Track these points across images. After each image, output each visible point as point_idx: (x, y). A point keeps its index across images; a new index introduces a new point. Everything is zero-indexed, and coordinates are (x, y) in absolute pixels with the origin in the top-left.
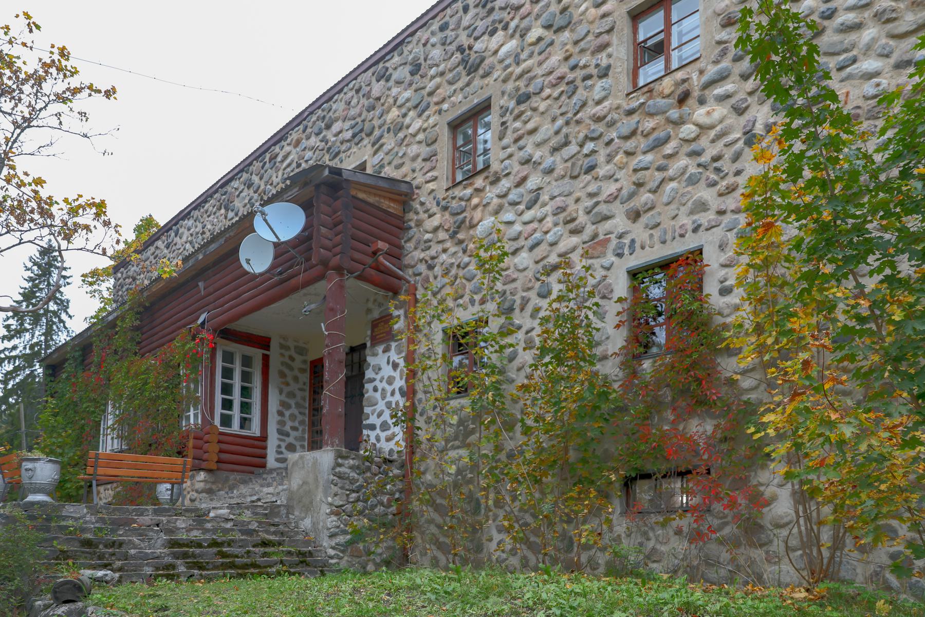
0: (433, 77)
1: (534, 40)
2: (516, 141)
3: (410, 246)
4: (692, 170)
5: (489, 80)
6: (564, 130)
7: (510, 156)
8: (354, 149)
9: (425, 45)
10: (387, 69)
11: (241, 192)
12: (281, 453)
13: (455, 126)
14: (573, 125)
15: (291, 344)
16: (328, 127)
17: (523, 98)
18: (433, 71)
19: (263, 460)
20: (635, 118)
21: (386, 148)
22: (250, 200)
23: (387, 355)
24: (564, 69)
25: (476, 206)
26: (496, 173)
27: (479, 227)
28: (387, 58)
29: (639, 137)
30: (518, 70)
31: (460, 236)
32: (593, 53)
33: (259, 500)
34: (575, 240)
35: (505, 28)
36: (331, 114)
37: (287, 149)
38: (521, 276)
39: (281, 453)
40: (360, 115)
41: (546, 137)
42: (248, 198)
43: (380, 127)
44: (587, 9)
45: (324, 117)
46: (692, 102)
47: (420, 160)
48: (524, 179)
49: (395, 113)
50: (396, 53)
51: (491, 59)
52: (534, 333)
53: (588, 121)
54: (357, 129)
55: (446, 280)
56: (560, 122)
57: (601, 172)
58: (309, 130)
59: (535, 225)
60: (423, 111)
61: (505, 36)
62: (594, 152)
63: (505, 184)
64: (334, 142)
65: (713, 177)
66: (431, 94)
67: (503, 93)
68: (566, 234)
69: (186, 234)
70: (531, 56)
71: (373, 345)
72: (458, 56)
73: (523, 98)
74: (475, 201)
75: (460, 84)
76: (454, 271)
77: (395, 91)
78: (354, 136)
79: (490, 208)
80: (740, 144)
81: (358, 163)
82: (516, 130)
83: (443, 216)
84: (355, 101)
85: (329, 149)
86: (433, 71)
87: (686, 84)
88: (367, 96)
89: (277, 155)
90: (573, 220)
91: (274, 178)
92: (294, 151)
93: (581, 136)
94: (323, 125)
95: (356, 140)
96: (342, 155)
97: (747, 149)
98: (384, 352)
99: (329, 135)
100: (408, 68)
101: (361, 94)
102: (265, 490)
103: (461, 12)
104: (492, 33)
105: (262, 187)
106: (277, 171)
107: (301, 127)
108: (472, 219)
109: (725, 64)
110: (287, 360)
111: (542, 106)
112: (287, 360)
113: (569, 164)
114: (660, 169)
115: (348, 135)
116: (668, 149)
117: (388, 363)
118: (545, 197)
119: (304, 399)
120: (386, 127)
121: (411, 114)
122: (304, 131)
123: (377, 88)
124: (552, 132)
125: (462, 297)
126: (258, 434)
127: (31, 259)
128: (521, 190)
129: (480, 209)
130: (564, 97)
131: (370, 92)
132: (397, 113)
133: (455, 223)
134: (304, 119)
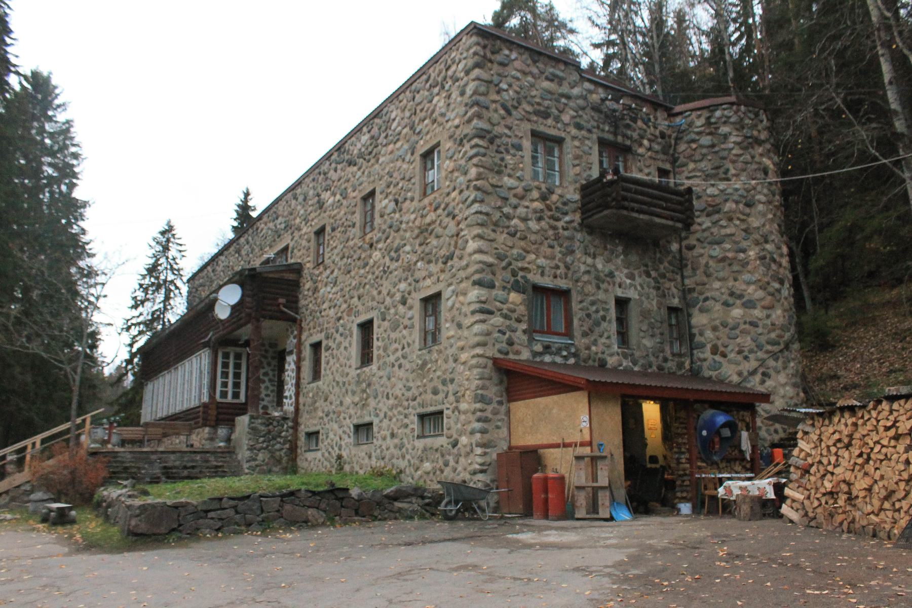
3: (301, 296)
15: (266, 343)
63: (328, 272)
69: (222, 265)
110: (263, 353)
112: (263, 353)
119: (274, 375)
127: (154, 239)
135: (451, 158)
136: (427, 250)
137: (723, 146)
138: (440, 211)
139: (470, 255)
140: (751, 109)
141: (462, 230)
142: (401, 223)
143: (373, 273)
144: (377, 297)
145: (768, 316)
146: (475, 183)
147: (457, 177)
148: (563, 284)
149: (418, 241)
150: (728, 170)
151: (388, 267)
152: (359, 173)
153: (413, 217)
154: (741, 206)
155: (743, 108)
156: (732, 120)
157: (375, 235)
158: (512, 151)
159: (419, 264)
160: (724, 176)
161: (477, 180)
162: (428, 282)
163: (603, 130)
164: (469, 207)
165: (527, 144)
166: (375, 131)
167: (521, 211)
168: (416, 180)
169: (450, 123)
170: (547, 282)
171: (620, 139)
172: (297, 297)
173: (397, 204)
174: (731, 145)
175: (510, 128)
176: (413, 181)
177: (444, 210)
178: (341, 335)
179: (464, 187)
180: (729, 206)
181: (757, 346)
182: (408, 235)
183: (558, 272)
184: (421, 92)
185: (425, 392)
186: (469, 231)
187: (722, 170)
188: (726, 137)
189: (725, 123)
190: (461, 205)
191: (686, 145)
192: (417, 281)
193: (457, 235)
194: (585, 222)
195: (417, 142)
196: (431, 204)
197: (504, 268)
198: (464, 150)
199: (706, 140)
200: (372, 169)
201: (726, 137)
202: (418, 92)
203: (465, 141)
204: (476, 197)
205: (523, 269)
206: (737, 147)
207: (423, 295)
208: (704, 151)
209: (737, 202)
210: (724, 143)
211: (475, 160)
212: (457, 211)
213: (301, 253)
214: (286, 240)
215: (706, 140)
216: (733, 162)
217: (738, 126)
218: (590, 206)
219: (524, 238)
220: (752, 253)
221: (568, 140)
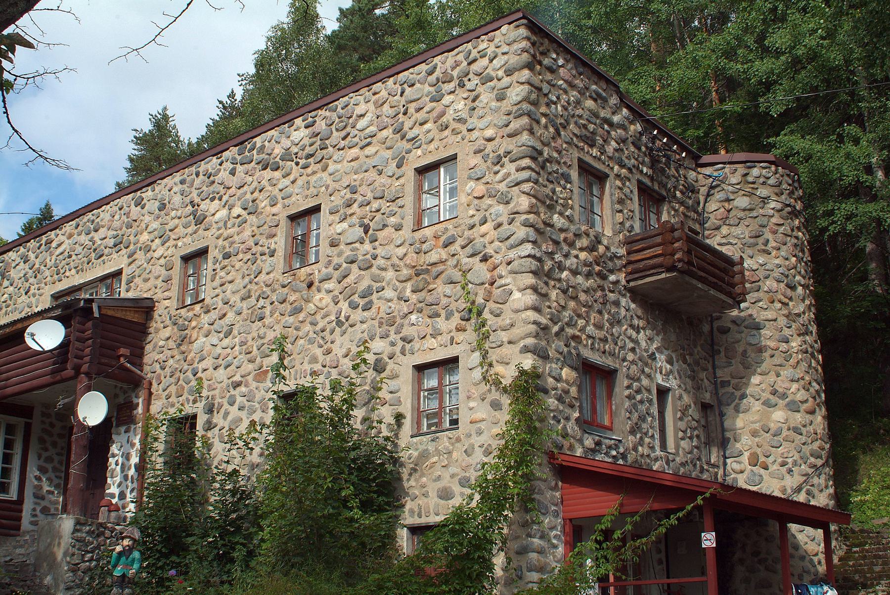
0: (173, 218)
1: (236, 216)
2: (221, 285)
3: (148, 348)
4: (311, 335)
5: (208, 233)
6: (249, 287)
7: (217, 296)
8: (115, 256)
9: (169, 191)
10: (143, 199)
11: (17, 265)
12: (35, 516)
13: (186, 259)
14: (254, 284)
16: (96, 231)
17: (227, 256)
18: (173, 213)
19: (16, 523)
20: (286, 290)
21: (138, 263)
22: (25, 275)
23: (127, 434)
24: (251, 243)
25: (194, 328)
26: (208, 306)
27: (195, 344)
28: (144, 190)
29: (288, 304)
30: (226, 233)
31: (183, 348)
32: (267, 238)
33: (11, 560)
34: (251, 366)
35: (220, 199)
36: (98, 220)
37: (62, 238)
38: (219, 386)
39: (35, 516)
40: (121, 229)
41: (238, 289)
42: (23, 272)
43: (134, 244)
44: (266, 206)
45: (93, 221)
46: (314, 288)
47: (161, 279)
48: (224, 315)
49: (145, 237)
50: (149, 188)
51: (211, 218)
52: (224, 431)
53: (262, 284)
54: (118, 240)
55: (173, 380)
56: (247, 280)
57: (267, 321)
58: (80, 228)
59: (229, 350)
60: (165, 242)
61: (220, 205)
62: (263, 307)
63: (214, 315)
64: (100, 245)
65: (321, 342)
66: (171, 230)
67: (216, 247)
68: (246, 362)
70: (234, 225)
71: (118, 426)
72: (190, 207)
73: (227, 256)
74: (194, 324)
75: (190, 230)
76: (178, 374)
77: (147, 218)
78: (115, 246)
79: (203, 331)
80: (334, 323)
81: (117, 268)
82: (221, 278)
83: (173, 329)
84: (117, 217)
85: (95, 250)
86: (173, 213)
87: (312, 276)
88: (127, 214)
89: (52, 241)
90: (250, 353)
91: (48, 261)
92: (67, 241)
93: (257, 294)
94: (92, 227)
95: (117, 248)
96: (104, 257)
97: (337, 328)
98: (125, 432)
99: (97, 236)
100: (157, 204)
101: (122, 212)
102: (18, 551)
103: (194, 176)
104: (213, 199)
105: (37, 266)
106: (51, 255)
107: (74, 223)
108: (191, 337)
109: (330, 269)
111: (238, 265)
113: (250, 311)
114: (297, 329)
115: (111, 242)
116: (301, 316)
117: (128, 442)
118: (235, 332)
120: (139, 245)
121: (158, 241)
122: (76, 228)
123: (135, 211)
124: (241, 286)
125: (181, 396)
126: (15, 498)
128: (222, 322)
129: (197, 329)
130: (249, 263)
131: (129, 213)
132: (147, 237)
133: (180, 337)
134: (78, 218)
135: (478, 179)
136: (430, 299)
138: (456, 247)
139: (517, 311)
140: (787, 172)
141: (501, 277)
142: (375, 257)
143: (314, 324)
144: (321, 358)
145: (811, 423)
146: (524, 217)
147: (490, 206)
148: (609, 362)
149: (409, 286)
151: (347, 318)
152: (287, 181)
153: (401, 251)
154: (782, 285)
156: (772, 181)
157: (317, 271)
158: (562, 182)
159: (413, 317)
160: (763, 248)
161: (529, 212)
162: (431, 342)
163: (642, 172)
164: (512, 247)
165: (574, 174)
166: (321, 125)
167: (571, 262)
168: (408, 200)
169: (475, 134)
170: (595, 358)
171: (656, 187)
172: (143, 348)
173: (366, 232)
175: (559, 152)
176: (400, 202)
177: (463, 247)
178: (241, 408)
179: (504, 219)
180: (770, 284)
181: (801, 458)
182: (390, 274)
184: (418, 85)
185: (425, 495)
186: (514, 279)
187: (761, 240)
188: (765, 200)
189: (764, 183)
190: (497, 243)
191: (718, 204)
192: (407, 340)
193: (492, 284)
194: (632, 284)
195: (409, 152)
196: (436, 237)
197: (557, 334)
198: (504, 171)
199: (742, 202)
200: (313, 179)
201: (765, 200)
202: (413, 85)
203: (505, 160)
204: (528, 235)
205: (574, 337)
206: (776, 214)
207: (420, 360)
208: (741, 214)
209: (779, 281)
210: (762, 208)
211: (527, 187)
212: (490, 250)
213: (149, 284)
214: (117, 262)
215: (742, 202)
216: (775, 232)
217: (776, 190)
219: (575, 298)
220: (794, 344)
221: (612, 176)
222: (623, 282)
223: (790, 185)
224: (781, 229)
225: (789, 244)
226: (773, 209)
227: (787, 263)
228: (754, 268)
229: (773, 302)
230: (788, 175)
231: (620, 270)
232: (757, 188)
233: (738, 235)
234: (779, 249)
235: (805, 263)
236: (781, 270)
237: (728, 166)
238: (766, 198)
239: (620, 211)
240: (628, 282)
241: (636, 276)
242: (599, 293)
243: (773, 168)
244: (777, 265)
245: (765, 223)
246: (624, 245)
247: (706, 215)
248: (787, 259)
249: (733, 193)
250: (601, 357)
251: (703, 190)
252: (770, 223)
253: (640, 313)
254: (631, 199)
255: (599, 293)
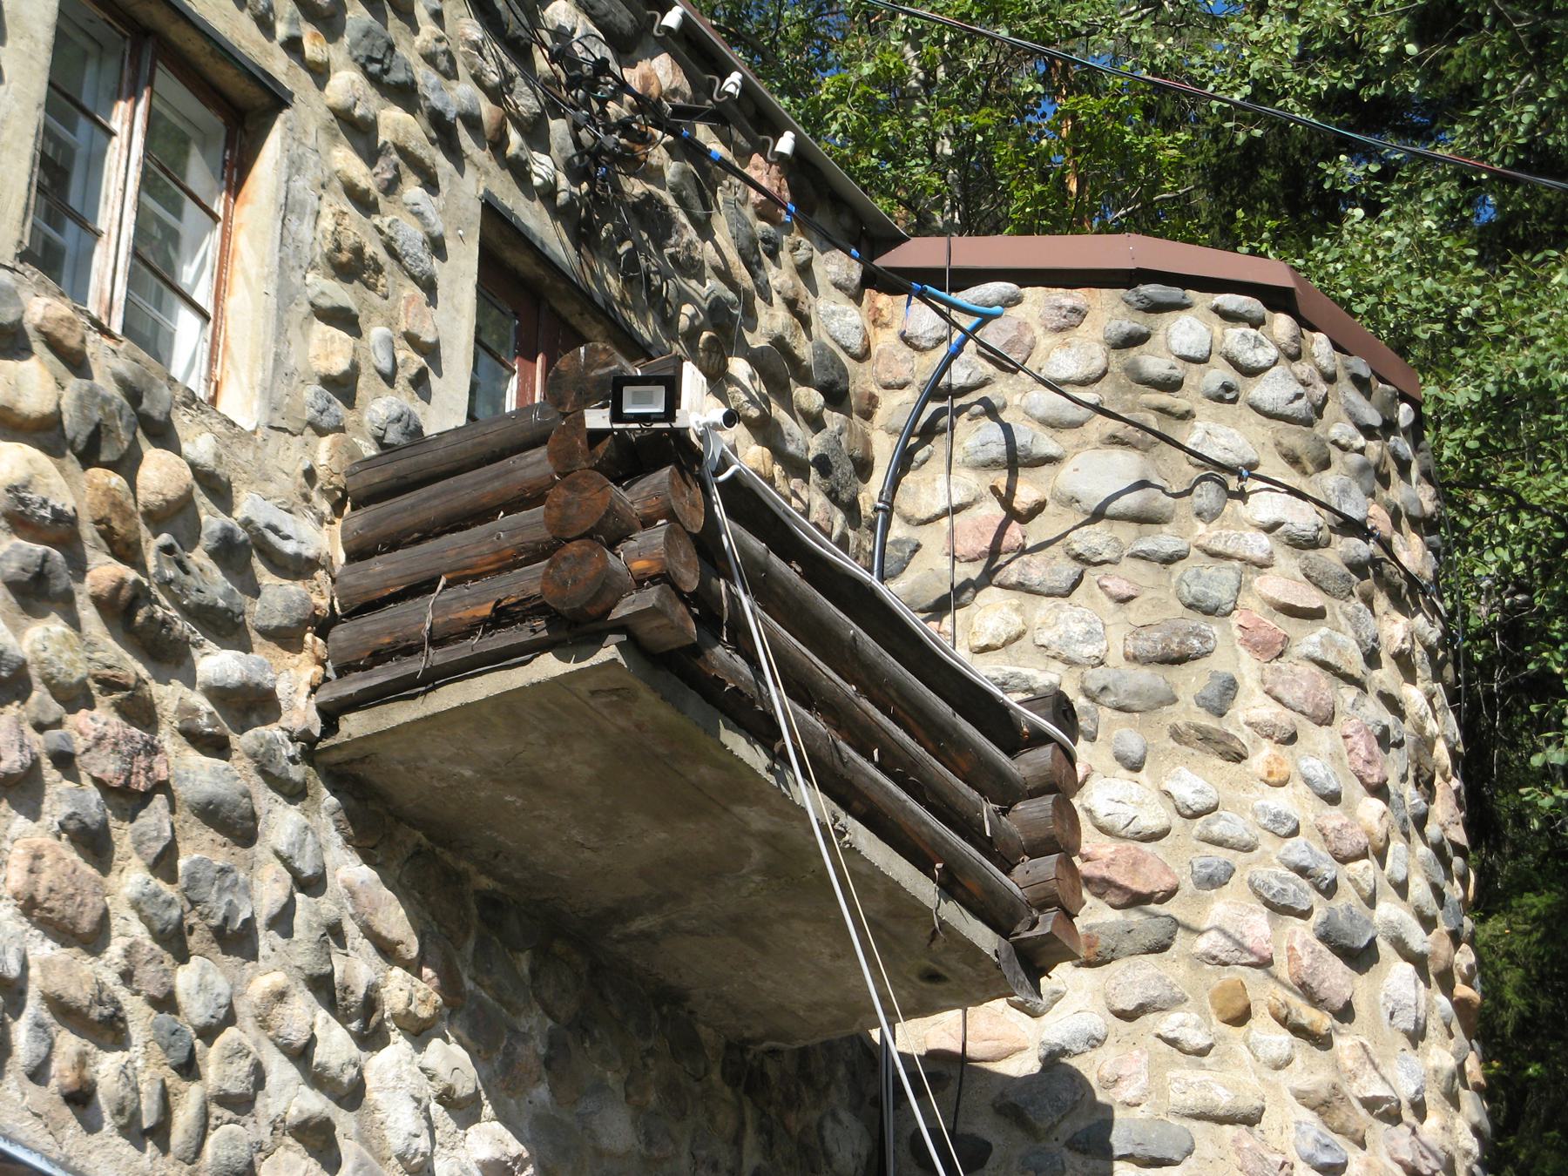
137: (1203, 532)
150: (1230, 688)
154: (1301, 933)
155: (1319, 343)
160: (1207, 721)
174: (1259, 545)
183: (107, 1067)
187: (1190, 681)
189: (1225, 395)
194: (354, 725)
206: (1288, 563)
209: (1280, 909)
216: (1275, 650)
217: (1295, 438)
218: (425, 614)
222: (301, 712)
223: (1368, 431)
224: (1310, 639)
225: (1342, 724)
226: (1270, 528)
227: (1333, 817)
228: (1151, 819)
229: (1241, 1018)
230: (1361, 383)
231: (286, 638)
232: (1186, 416)
233: (1069, 640)
234: (1292, 739)
235: (1439, 849)
236: (1297, 850)
237: (1032, 294)
238: (1231, 470)
239: (343, 319)
240: (330, 715)
241: (379, 676)
242: (100, 719)
243: (1282, 324)
244: (1277, 818)
245: (1220, 593)
246: (338, 508)
247: (898, 530)
248: (1333, 798)
249: (1055, 425)
250: (54, 1129)
251: (895, 407)
252: (1246, 600)
253: (395, 920)
254: (429, 286)
255: (100, 719)
